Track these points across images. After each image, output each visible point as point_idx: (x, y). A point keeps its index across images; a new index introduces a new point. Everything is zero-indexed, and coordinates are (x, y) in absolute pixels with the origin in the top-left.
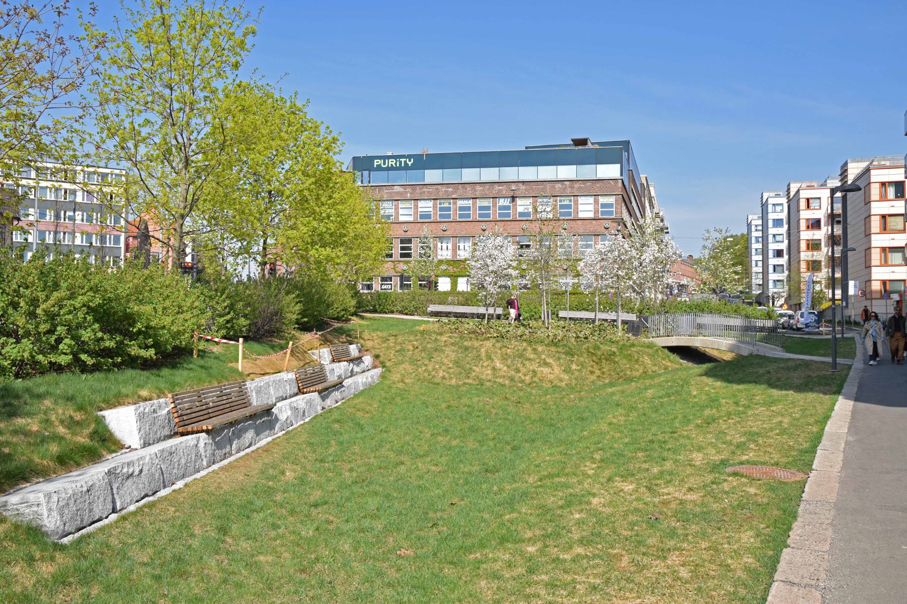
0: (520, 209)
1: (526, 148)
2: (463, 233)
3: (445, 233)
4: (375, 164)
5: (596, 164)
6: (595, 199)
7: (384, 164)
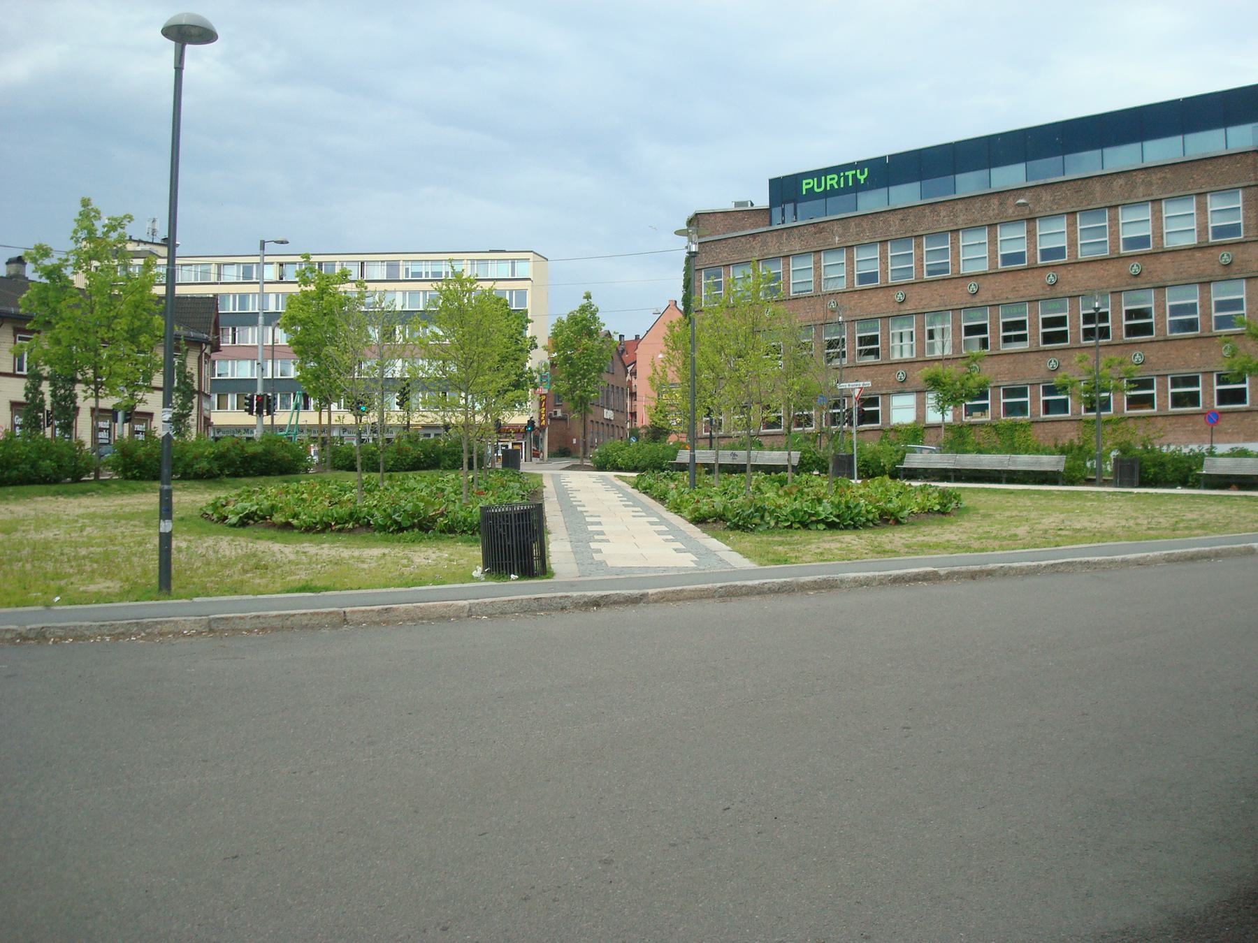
0: (1127, 233)
1: (737, 204)
2: (934, 304)
3: (902, 307)
4: (805, 187)
5: (1064, 154)
6: (1198, 202)
7: (819, 186)
